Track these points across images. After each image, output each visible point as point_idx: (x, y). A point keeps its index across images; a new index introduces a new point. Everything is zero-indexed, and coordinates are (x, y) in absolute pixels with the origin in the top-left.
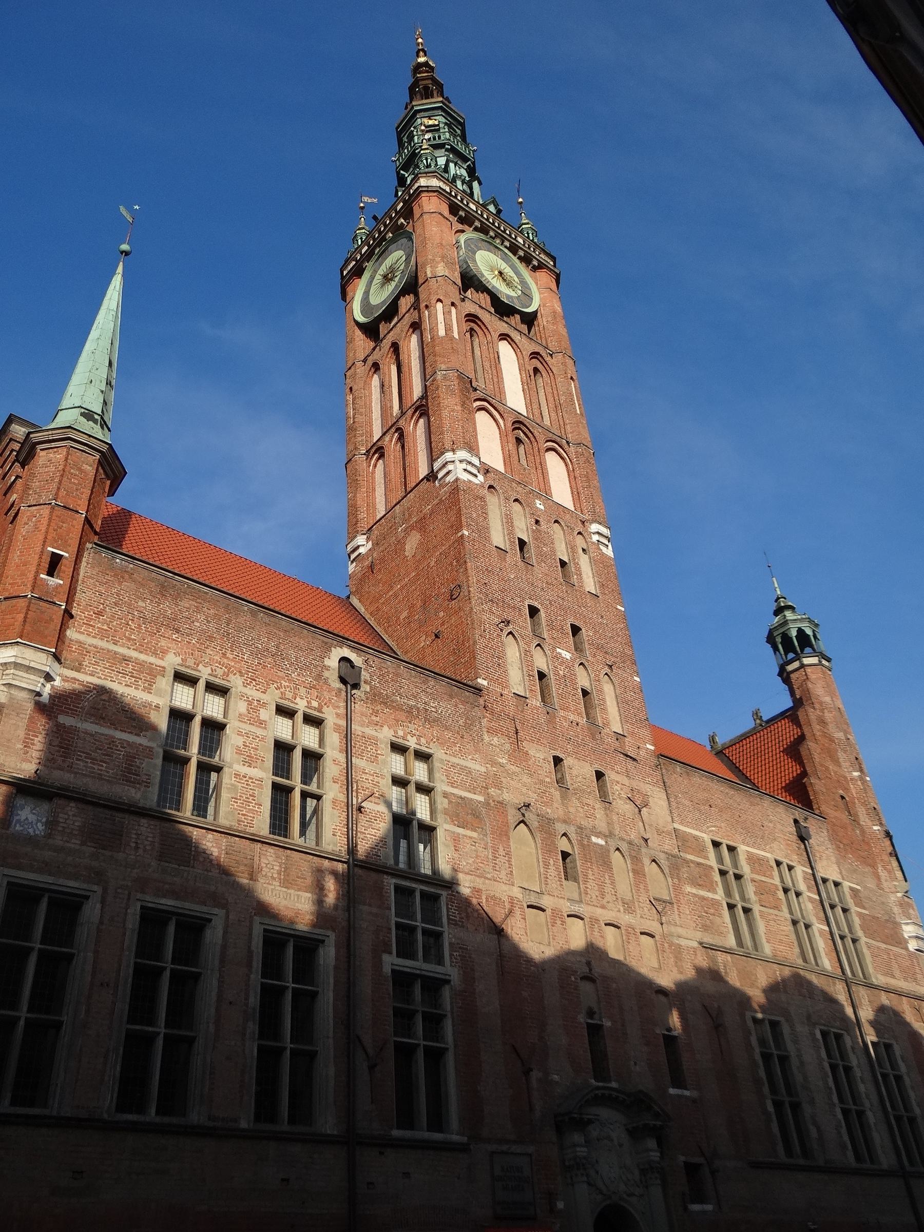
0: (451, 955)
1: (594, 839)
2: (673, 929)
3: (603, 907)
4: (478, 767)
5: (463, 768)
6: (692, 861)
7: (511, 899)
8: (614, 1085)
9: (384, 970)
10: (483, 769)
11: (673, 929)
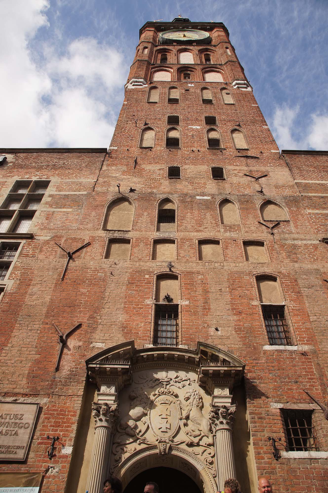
1: (198, 197)
2: (287, 236)
3: (198, 231)
4: (89, 180)
5: (73, 183)
6: (314, 197)
7: (93, 238)
10: (94, 180)
11: (287, 236)
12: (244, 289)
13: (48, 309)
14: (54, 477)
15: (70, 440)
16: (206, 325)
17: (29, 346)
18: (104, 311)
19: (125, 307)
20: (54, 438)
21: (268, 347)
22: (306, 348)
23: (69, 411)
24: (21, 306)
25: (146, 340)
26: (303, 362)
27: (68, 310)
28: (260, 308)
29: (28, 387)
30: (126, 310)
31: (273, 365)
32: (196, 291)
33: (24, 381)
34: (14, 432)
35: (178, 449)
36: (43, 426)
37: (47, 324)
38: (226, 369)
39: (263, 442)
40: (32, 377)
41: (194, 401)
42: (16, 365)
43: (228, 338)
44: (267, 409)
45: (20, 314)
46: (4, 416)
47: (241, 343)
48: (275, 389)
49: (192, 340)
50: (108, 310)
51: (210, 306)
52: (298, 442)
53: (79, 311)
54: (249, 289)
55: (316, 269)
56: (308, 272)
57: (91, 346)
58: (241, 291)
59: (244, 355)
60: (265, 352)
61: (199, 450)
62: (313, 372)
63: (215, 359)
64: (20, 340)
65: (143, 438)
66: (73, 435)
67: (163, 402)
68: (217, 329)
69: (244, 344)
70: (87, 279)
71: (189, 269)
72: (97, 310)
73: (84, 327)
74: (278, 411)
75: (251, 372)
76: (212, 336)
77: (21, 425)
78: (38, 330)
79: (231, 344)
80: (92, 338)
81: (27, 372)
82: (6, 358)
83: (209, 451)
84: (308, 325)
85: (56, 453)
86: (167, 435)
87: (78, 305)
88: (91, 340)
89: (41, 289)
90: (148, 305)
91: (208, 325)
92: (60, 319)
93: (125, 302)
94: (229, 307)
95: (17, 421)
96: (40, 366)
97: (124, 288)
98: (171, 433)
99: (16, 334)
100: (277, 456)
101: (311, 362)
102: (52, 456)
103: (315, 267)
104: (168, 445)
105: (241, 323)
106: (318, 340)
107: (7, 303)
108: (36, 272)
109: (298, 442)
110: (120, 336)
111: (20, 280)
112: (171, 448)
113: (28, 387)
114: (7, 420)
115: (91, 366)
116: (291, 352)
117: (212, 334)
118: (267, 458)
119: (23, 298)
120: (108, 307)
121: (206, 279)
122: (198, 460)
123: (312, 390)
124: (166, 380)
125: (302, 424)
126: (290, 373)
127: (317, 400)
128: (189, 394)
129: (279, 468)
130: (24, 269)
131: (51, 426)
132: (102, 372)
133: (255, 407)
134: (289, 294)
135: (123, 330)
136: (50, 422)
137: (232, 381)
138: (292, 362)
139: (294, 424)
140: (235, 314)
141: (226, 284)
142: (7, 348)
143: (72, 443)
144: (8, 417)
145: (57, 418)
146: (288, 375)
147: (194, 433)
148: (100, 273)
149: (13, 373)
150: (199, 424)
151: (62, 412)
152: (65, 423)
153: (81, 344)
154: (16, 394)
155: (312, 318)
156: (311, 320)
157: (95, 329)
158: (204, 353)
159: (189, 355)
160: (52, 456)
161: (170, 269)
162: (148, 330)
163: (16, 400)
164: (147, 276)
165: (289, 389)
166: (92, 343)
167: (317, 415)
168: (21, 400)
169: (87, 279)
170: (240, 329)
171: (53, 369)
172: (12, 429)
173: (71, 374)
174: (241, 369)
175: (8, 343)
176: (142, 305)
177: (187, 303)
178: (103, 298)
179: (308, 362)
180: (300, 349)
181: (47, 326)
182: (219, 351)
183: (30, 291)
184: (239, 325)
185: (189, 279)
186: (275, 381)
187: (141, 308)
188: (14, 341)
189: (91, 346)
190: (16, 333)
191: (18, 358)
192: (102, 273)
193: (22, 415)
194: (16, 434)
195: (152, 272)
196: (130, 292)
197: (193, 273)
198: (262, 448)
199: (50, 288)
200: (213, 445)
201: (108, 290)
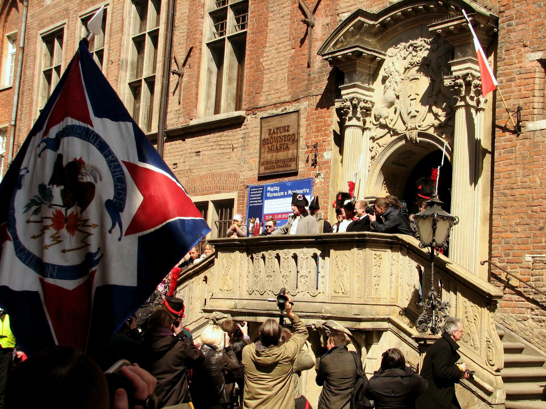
33: (286, 88)
34: (285, 147)
36: (307, 133)
38: (455, 23)
40: (292, 80)
42: (277, 68)
44: (520, 64)
48: (535, 30)
64: (275, 35)
67: (412, 78)
78: (288, 14)
80: (338, 7)
82: (268, 62)
86: (417, 119)
95: (286, 134)
99: (271, 28)
114: (279, 135)
129: (520, 145)
133: (505, 64)
136: (312, 129)
142: (266, 50)
149: (276, 80)
153: (328, 20)
166: (338, 15)
172: (283, 143)
173: (323, 66)
186: (539, 17)
189: (338, 19)
191: (278, 60)
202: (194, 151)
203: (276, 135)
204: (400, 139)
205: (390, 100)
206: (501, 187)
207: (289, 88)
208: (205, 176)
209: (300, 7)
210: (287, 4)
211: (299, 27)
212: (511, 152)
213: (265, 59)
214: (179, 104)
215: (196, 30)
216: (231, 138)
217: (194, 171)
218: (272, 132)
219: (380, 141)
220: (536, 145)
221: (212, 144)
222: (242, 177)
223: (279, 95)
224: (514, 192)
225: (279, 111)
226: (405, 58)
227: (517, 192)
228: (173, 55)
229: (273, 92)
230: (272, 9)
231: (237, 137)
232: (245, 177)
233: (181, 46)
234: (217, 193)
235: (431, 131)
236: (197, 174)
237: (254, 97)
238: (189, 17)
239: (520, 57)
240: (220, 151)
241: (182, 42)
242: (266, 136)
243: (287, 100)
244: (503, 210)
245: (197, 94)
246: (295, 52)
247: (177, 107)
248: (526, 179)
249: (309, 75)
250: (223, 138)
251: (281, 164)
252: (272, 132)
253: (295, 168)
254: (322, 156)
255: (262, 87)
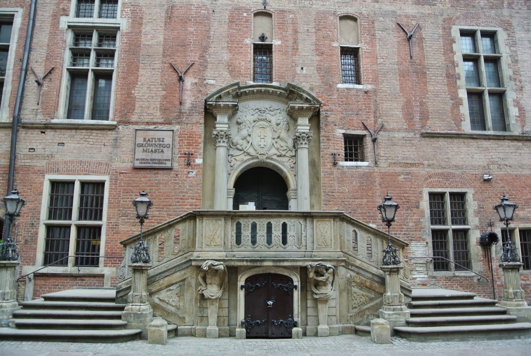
0: (122, 11)
8: (274, 84)
9: (61, 26)
12: (328, 30)
13: (164, 48)
14: (194, 178)
15: (200, 154)
16: (294, 64)
17: (156, 84)
18: (211, 50)
19: (228, 47)
20: (189, 154)
21: (340, 86)
22: (369, 87)
23: (195, 135)
24: (139, 46)
25: (247, 77)
26: (365, 99)
27: (181, 49)
28: (339, 50)
29: (162, 118)
30: (230, 49)
31: (342, 100)
32: (287, 31)
33: (158, 114)
34: (160, 151)
35: (272, 159)
36: (180, 146)
37: (166, 63)
38: (307, 105)
39: (328, 156)
40: (164, 110)
41: (283, 125)
43: (311, 76)
45: (141, 54)
46: (151, 140)
47: (320, 81)
48: (341, 119)
49: (282, 77)
50: (214, 49)
51: (298, 46)
52: (351, 155)
53: (191, 50)
54: (332, 30)
55: (393, 11)
56: (385, 14)
57: (205, 82)
58: (325, 32)
59: (321, 92)
60: (338, 89)
61: (285, 159)
62: (370, 107)
63: (301, 97)
65: (248, 151)
66: (201, 151)
68: (302, 68)
69: (323, 82)
70: (192, 17)
71: (281, 7)
72: (205, 49)
73: (196, 65)
74: (341, 135)
75: (325, 105)
76: (299, 74)
77: (164, 145)
79: (313, 81)
81: (159, 106)
82: (140, 94)
83: (292, 160)
84: (375, 67)
85: (192, 163)
86: (264, 150)
87: (189, 45)
88: (204, 78)
89: (153, 28)
90: (248, 44)
91: (296, 65)
92: (176, 58)
93: (228, 41)
94: (313, 47)
95: (161, 143)
96: (168, 100)
97: (226, 27)
98: (266, 149)
100: (335, 164)
101: (371, 99)
102: (189, 164)
103: (393, 8)
104: (265, 156)
105: (322, 64)
106: (380, 81)
107: (126, 43)
108: (144, 9)
109: (351, 155)
110: (226, 73)
111: (131, 18)
112: (267, 158)
113: (162, 118)
114: (154, 142)
115: (209, 103)
116: (357, 90)
117: (299, 72)
118: (329, 165)
119: (139, 38)
120: (214, 46)
121: (296, 19)
122: (284, 166)
123: (367, 120)
124: (264, 109)
125: (356, 143)
126: (354, 107)
127: (368, 128)
128: (280, 121)
130: (132, 5)
131: (185, 145)
132: (217, 107)
133: (325, 131)
134: (364, 37)
135: (228, 68)
137: (310, 114)
138: (357, 98)
139: (350, 143)
140: (318, 55)
141: (313, 25)
143: (202, 157)
144: (154, 140)
145: (188, 140)
146: (352, 109)
147: (283, 148)
148: (203, 10)
150: (287, 143)
151: (191, 136)
152: (195, 143)
153: (196, 81)
154: (154, 123)
155: (380, 61)
156: (378, 62)
157: (206, 67)
158: (291, 92)
159: (280, 91)
160: (189, 164)
161: (265, 7)
162: (249, 69)
163: (155, 128)
164: (245, 14)
165: (350, 120)
166: (205, 80)
167: (367, 138)
168: (160, 127)
169: (192, 17)
170: (320, 68)
171: (178, 103)
174: (318, 106)
175: (137, 81)
176: (242, 44)
177: (279, 43)
178: (209, 37)
179: (369, 99)
180: (365, 88)
181: (165, 65)
182: (304, 91)
183: (143, 31)
184: (320, 65)
185: (281, 18)
187: (242, 47)
188: (142, 79)
189: (205, 82)
190: (141, 72)
191: (149, 95)
192: (205, 10)
193: (164, 139)
194: (162, 151)
195: (249, 10)
196: (231, 31)
197: (285, 11)
198: (326, 160)
199: (161, 27)
200: (295, 156)
201: (212, 29)
202: (56, 141)
203: (151, 143)
204: (252, 159)
205: (245, 136)
206: (327, 191)
207: (161, 114)
208: (72, 162)
209: (172, 66)
210: (157, 62)
211: (170, 79)
212: (331, 174)
213: (136, 92)
214: (38, 104)
215: (58, 57)
216: (101, 138)
217: (56, 156)
218: (147, 140)
219: (237, 158)
220: (344, 173)
221: (78, 139)
222: (113, 166)
223: (152, 117)
224: (334, 194)
225: (152, 127)
226: (253, 115)
227: (335, 194)
228: (30, 69)
229: (146, 114)
230: (143, 62)
231: (109, 138)
232: (117, 167)
233: (39, 64)
234: (84, 174)
235: (275, 157)
236: (60, 159)
237: (126, 114)
238: (48, 45)
239: (333, 130)
240: (88, 145)
241: (40, 61)
242: (140, 140)
243: (159, 122)
244: (328, 202)
245: (58, 101)
246: (167, 93)
247: (36, 107)
248: (340, 189)
249: (181, 110)
250: (91, 137)
251: (156, 162)
252: (147, 140)
253: (170, 165)
254: (194, 161)
255: (134, 110)
